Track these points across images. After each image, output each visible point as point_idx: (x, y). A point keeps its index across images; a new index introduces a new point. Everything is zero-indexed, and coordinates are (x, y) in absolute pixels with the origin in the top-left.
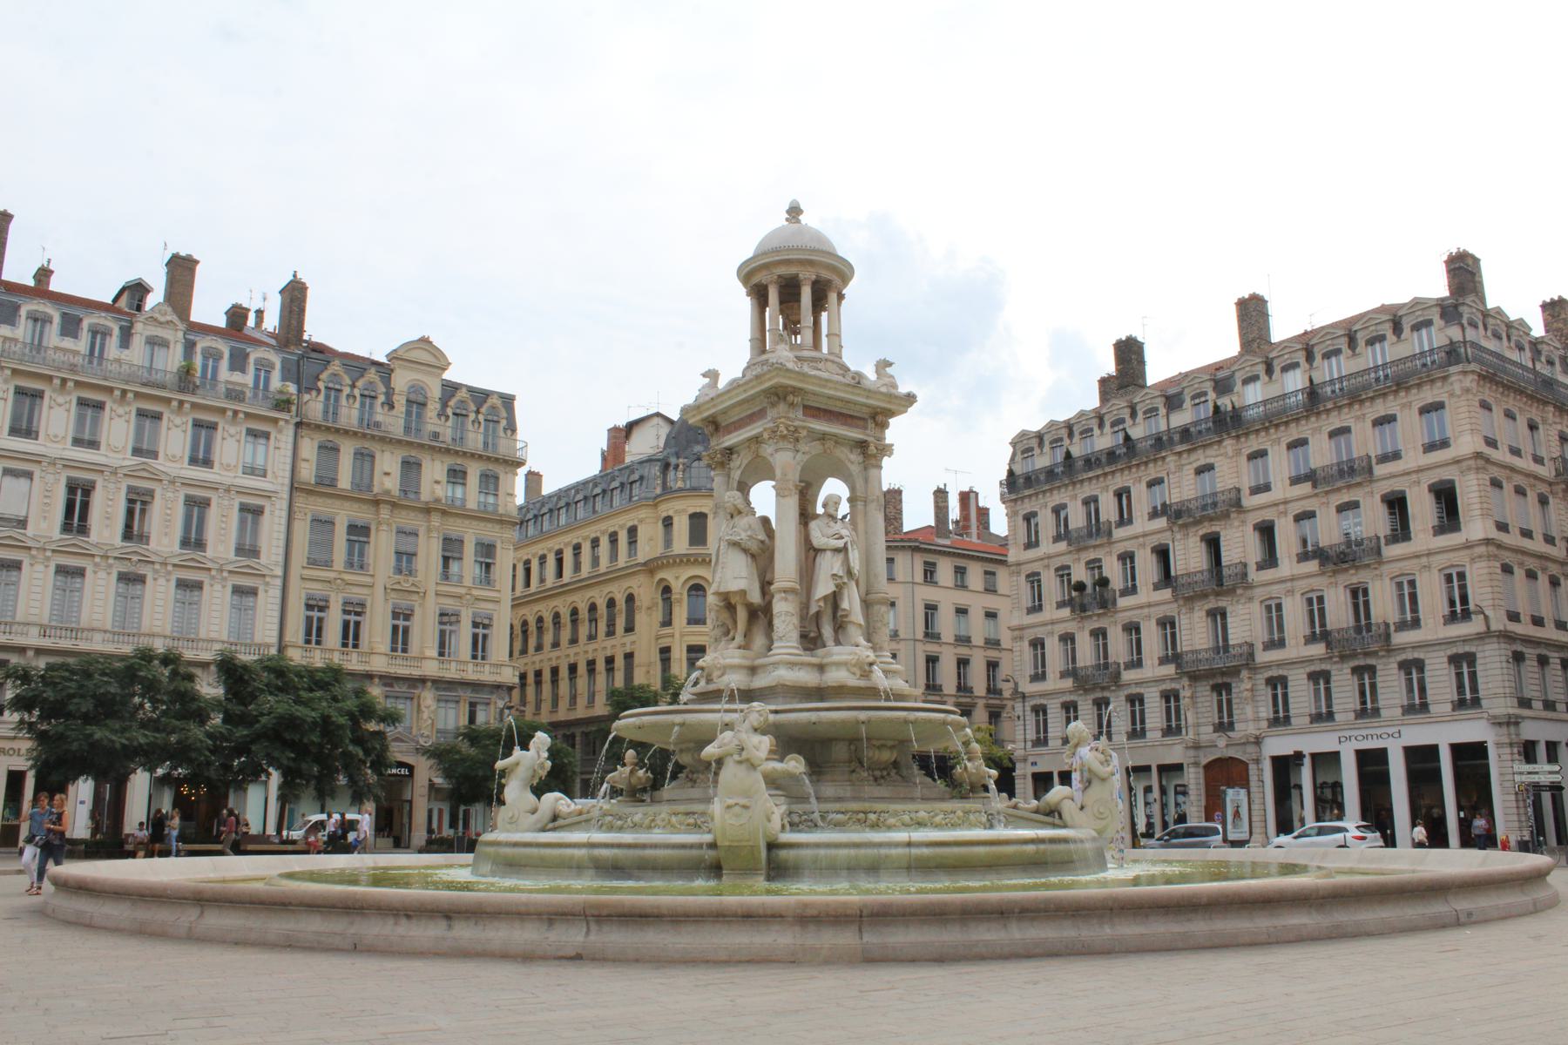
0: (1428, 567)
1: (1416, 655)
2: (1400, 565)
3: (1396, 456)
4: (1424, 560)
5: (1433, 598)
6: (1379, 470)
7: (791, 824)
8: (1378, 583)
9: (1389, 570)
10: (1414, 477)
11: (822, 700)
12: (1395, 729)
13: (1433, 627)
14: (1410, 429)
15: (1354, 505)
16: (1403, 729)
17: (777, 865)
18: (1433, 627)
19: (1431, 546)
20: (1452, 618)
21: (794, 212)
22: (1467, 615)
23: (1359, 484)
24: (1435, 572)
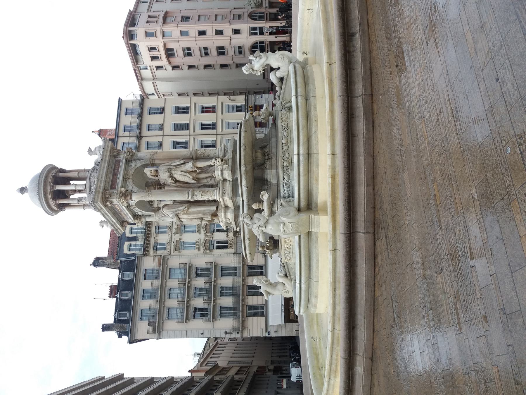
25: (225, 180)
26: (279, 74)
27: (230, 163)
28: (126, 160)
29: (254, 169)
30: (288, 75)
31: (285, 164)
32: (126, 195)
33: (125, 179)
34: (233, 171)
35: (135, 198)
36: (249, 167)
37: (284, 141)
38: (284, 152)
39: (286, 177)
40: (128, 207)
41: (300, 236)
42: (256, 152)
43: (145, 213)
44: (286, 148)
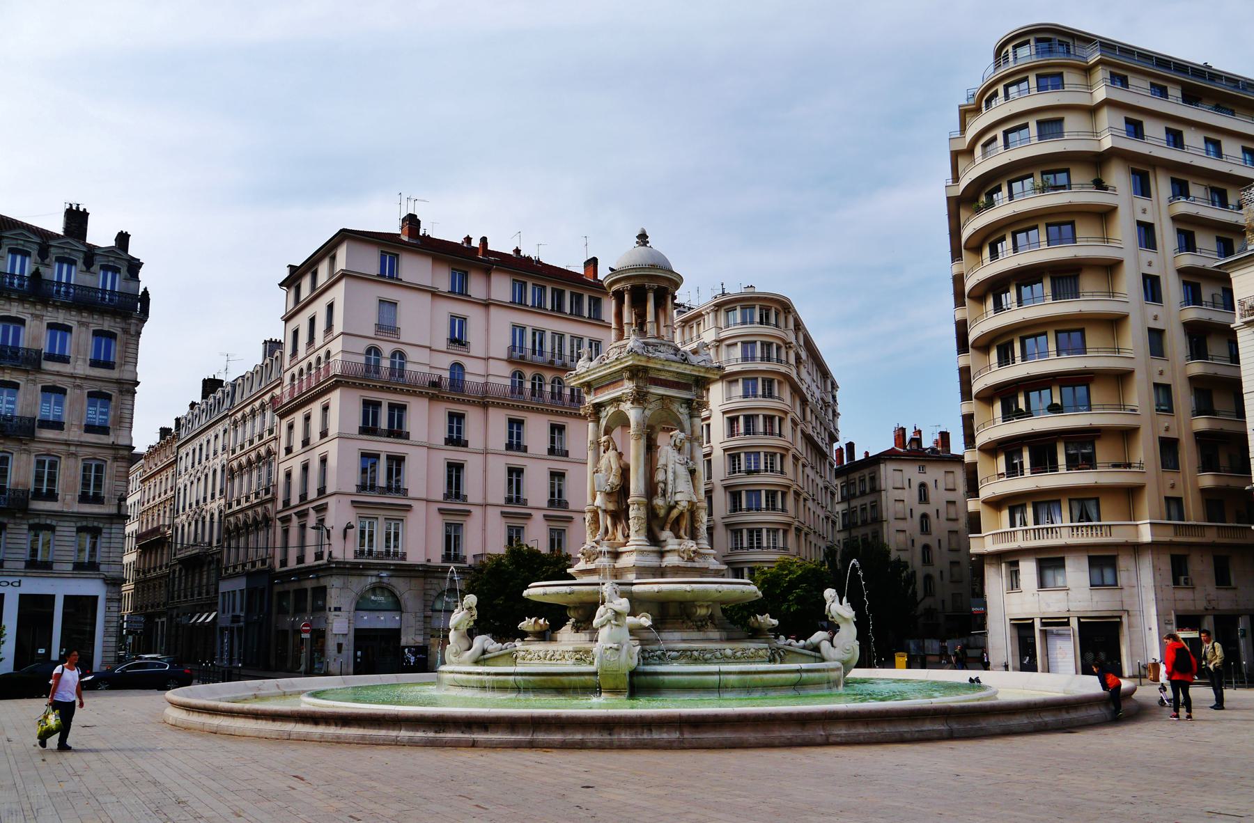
0: (74, 455)
1: (96, 524)
2: (49, 446)
3: (64, 359)
4: (73, 449)
5: (69, 475)
6: (47, 365)
7: (644, 658)
8: (24, 457)
9: (35, 447)
10: (78, 382)
11: (662, 577)
12: (17, 579)
13: (68, 501)
14: (81, 342)
15: (16, 386)
16: (24, 580)
17: (638, 685)
18: (68, 501)
19: (83, 439)
20: (84, 498)
21: (643, 238)
22: (98, 499)
23: (27, 372)
24: (80, 459)
25: (662, 554)
26: (825, 646)
27: (689, 564)
28: (692, 400)
29: (681, 603)
30: (823, 660)
31: (696, 653)
32: (639, 398)
33: (662, 397)
34: (676, 571)
35: (633, 413)
36: (689, 596)
37: (729, 652)
38: (711, 651)
39: (674, 654)
40: (617, 400)
41: (595, 674)
42: (708, 607)
43: (603, 423)
44: (718, 654)
